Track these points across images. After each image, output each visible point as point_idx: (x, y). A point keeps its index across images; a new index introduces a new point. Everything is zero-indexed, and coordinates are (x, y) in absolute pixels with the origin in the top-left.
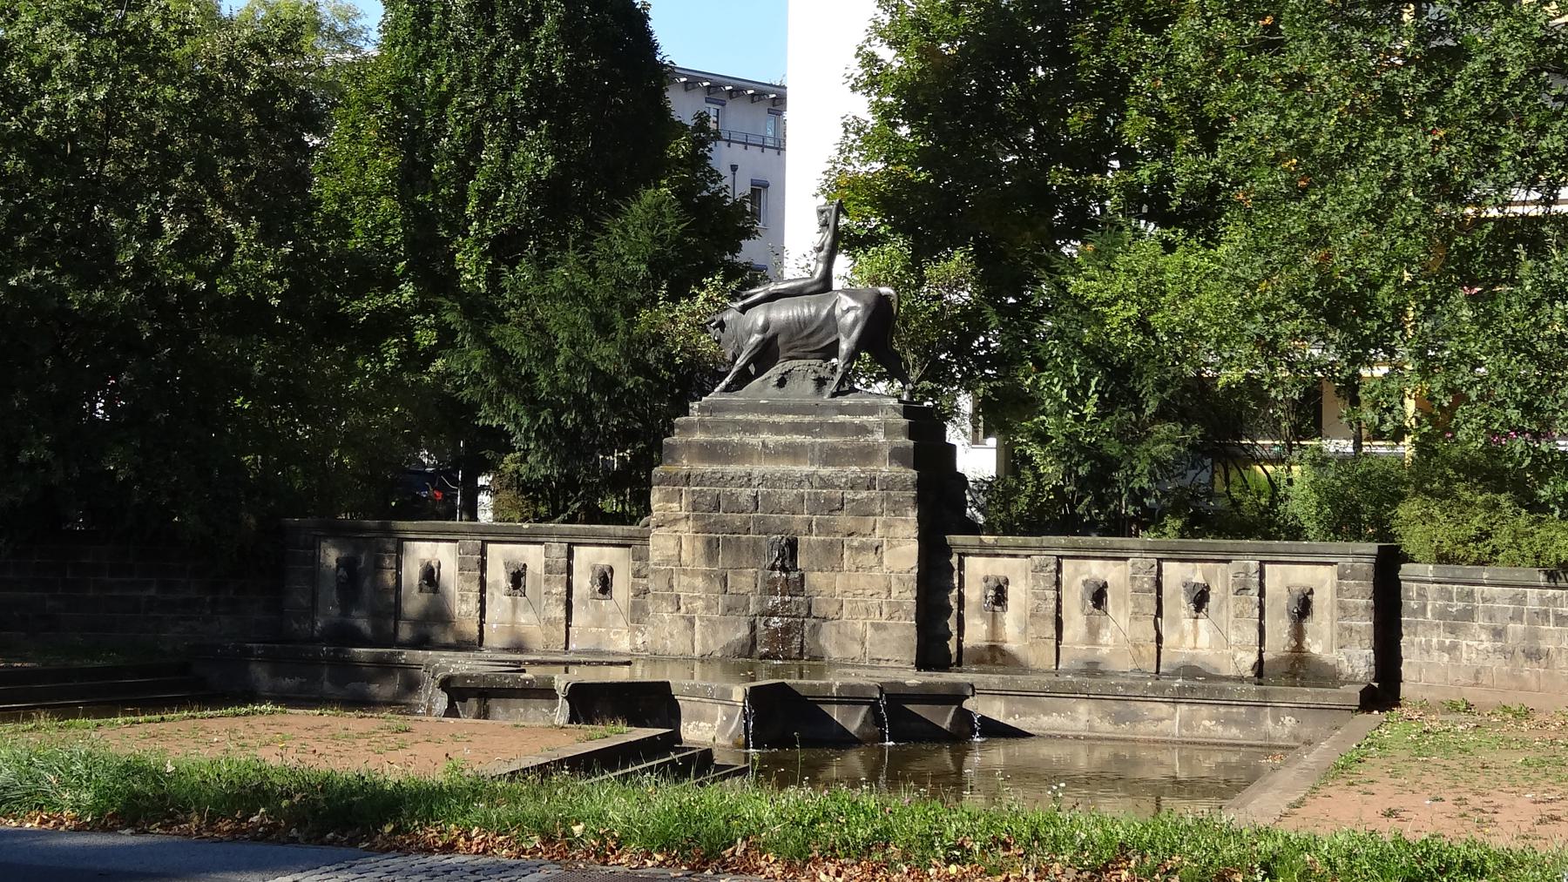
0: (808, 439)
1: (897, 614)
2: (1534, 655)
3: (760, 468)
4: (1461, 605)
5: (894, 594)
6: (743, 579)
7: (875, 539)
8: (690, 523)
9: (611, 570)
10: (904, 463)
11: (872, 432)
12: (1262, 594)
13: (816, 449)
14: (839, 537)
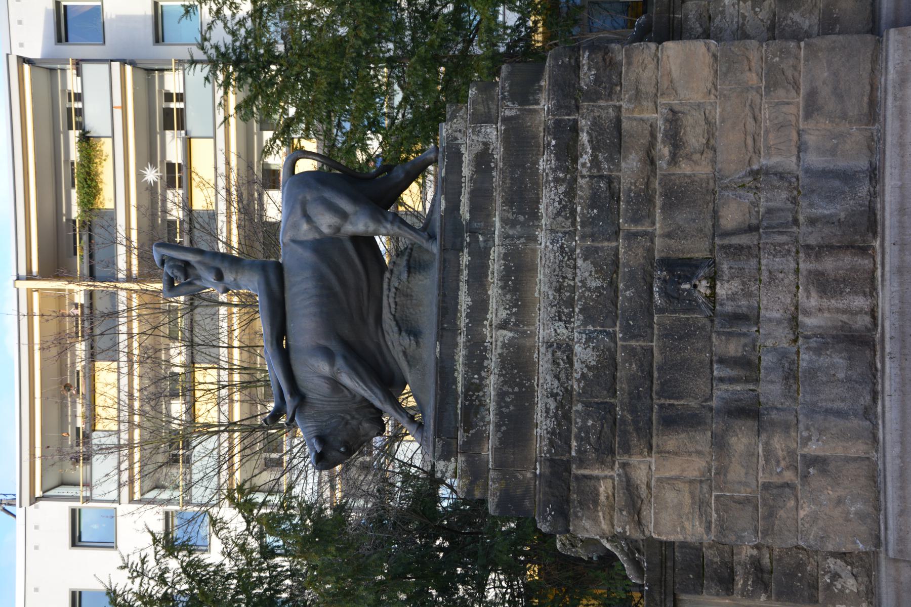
0: (496, 251)
1: (789, 73)
8: (634, 460)
10: (538, 76)
11: (486, 145)
13: (511, 232)
14: (656, 185)
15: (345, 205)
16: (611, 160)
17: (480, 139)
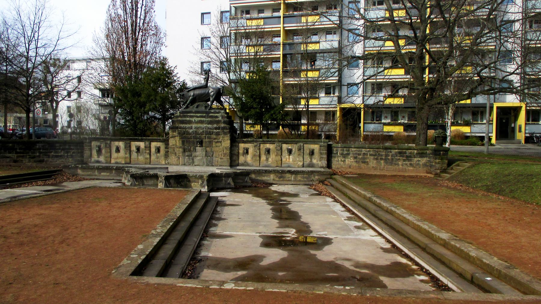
3: (194, 126)
4: (346, 152)
5: (225, 151)
7: (220, 140)
9: (160, 147)
10: (227, 124)
12: (303, 150)
15: (214, 97)
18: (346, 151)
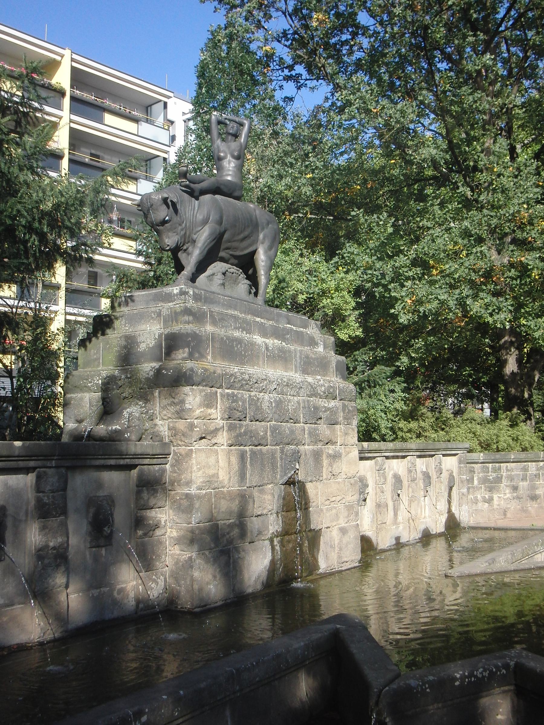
2: (534, 498)
4: (494, 475)
6: (266, 497)
8: (225, 433)
16: (327, 419)
17: (319, 341)
18: (495, 470)
